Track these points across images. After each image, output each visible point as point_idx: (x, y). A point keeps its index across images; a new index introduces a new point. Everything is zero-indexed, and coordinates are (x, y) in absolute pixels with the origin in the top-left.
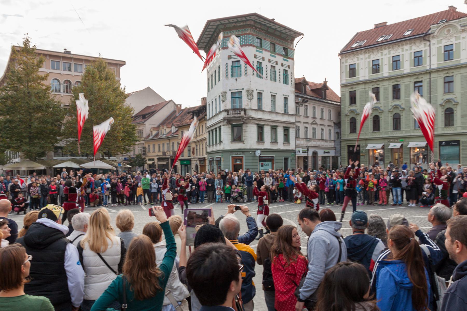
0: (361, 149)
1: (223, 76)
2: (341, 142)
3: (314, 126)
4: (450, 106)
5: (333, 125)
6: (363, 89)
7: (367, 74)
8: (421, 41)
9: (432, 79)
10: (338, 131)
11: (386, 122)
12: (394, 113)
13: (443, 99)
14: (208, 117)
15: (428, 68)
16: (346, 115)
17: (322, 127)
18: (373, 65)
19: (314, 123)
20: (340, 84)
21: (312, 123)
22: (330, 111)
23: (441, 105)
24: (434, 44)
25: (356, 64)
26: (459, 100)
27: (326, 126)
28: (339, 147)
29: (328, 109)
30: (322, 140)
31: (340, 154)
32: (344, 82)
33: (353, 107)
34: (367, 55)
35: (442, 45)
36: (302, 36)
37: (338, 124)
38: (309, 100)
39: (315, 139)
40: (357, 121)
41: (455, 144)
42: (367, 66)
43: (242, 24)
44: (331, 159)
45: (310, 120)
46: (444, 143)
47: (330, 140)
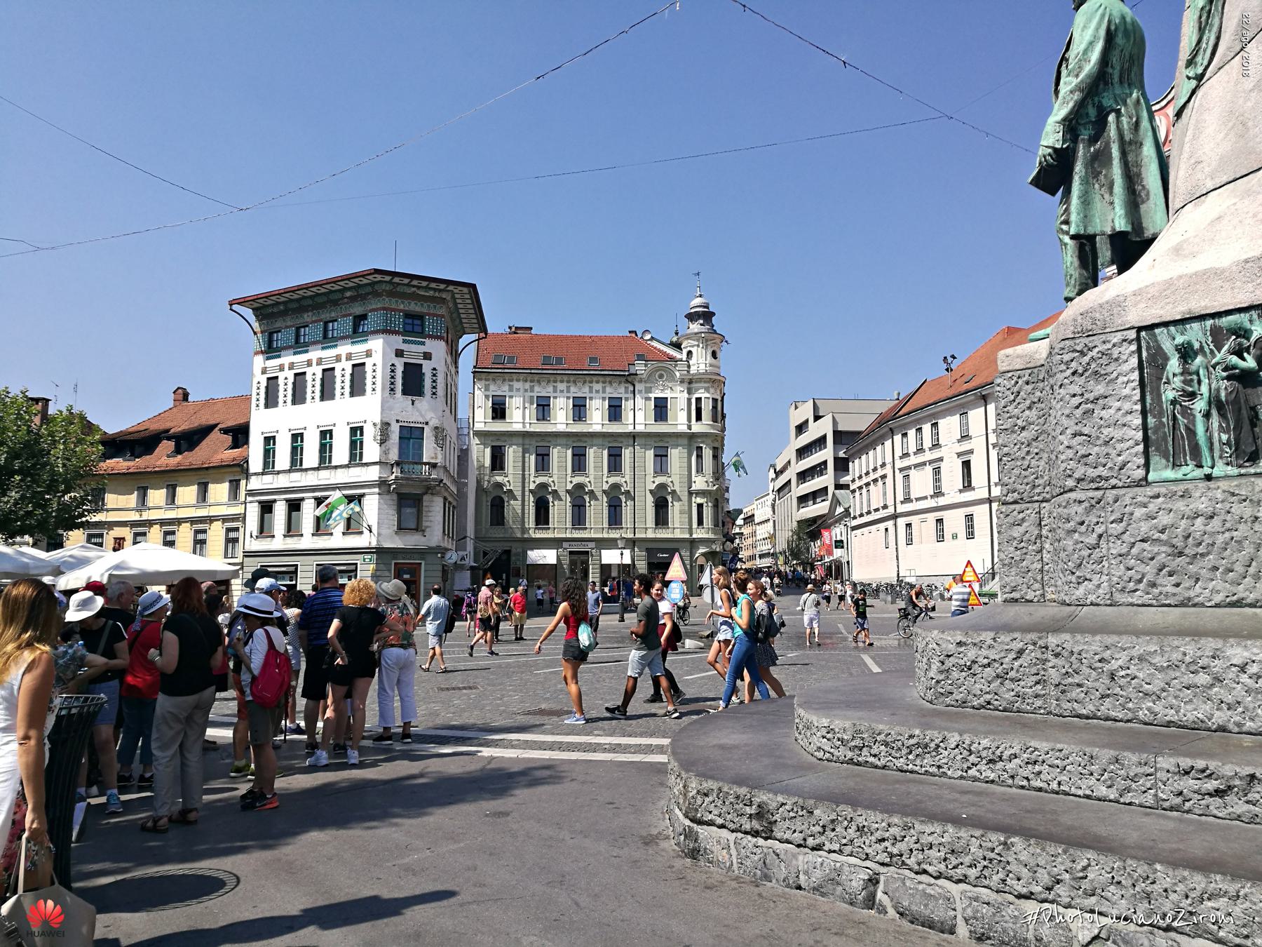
0: (513, 558)
1: (383, 389)
11: (560, 511)
14: (256, 464)
15: (630, 429)
23: (651, 491)
32: (479, 426)
34: (527, 385)
43: (431, 293)
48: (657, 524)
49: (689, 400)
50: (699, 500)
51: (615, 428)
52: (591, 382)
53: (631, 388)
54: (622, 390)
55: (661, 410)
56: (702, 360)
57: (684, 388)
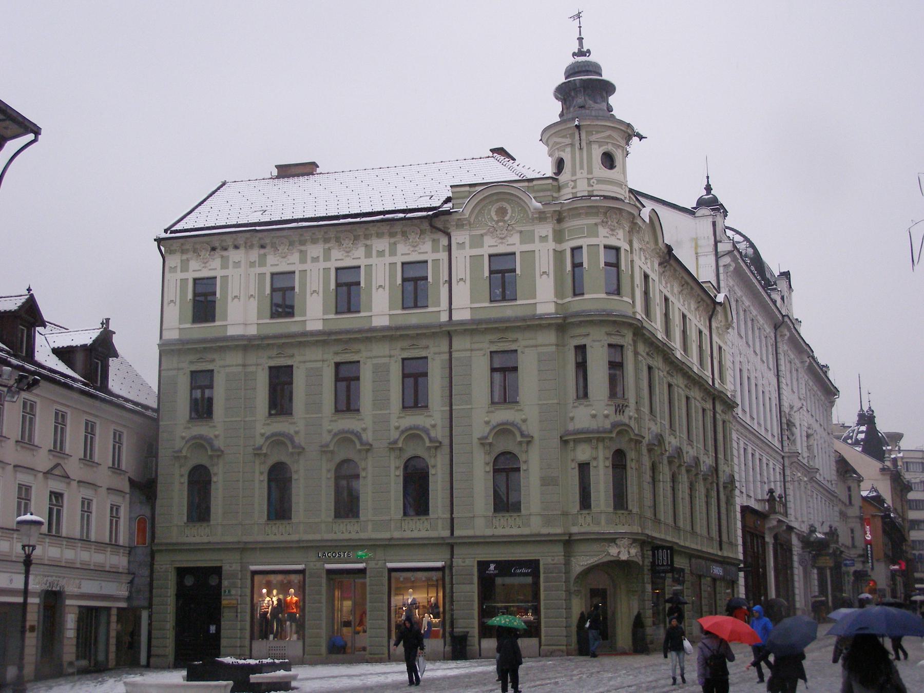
0: (225, 583)
2: (152, 555)
3: (56, 485)
4: (510, 446)
5: (126, 487)
6: (240, 369)
7: (253, 317)
8: (422, 232)
9: (454, 355)
10: (147, 511)
12: (338, 459)
13: (487, 423)
16: (177, 457)
17: (87, 493)
18: (273, 290)
19: (56, 472)
20: (158, 341)
21: (48, 474)
22: (118, 438)
23: (483, 442)
24: (461, 245)
25: (218, 280)
26: (533, 427)
27: (103, 491)
28: (146, 572)
29: (113, 427)
30: (85, 541)
31: (151, 599)
32: (172, 335)
33: (201, 429)
34: (254, 255)
35: (486, 251)
36: (31, 137)
37: (145, 488)
38: (43, 383)
39: (59, 536)
40: (214, 479)
41: (524, 570)
42: (253, 290)
44: (114, 618)
45: (43, 461)
46: (492, 567)
47: (113, 545)
48: (495, 510)
49: (559, 255)
50: (583, 453)
51: (415, 317)
52: (367, 237)
53: (444, 241)
54: (427, 246)
55: (502, 276)
56: (582, 174)
57: (546, 229)
